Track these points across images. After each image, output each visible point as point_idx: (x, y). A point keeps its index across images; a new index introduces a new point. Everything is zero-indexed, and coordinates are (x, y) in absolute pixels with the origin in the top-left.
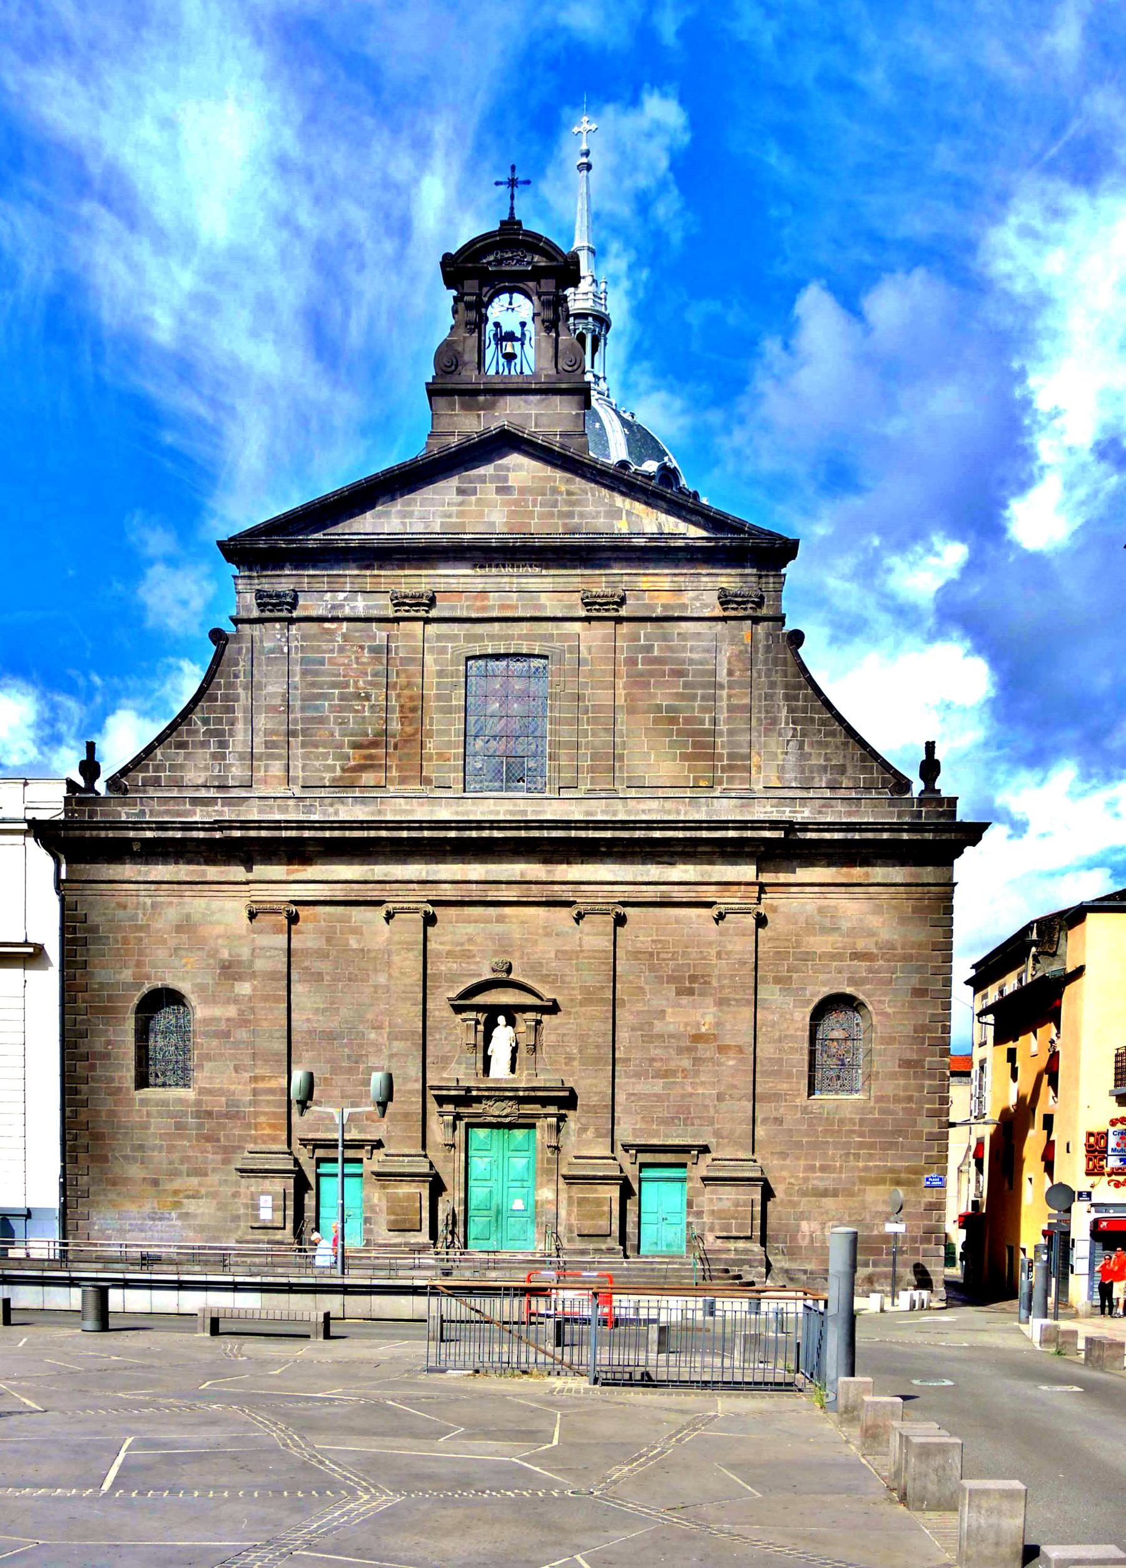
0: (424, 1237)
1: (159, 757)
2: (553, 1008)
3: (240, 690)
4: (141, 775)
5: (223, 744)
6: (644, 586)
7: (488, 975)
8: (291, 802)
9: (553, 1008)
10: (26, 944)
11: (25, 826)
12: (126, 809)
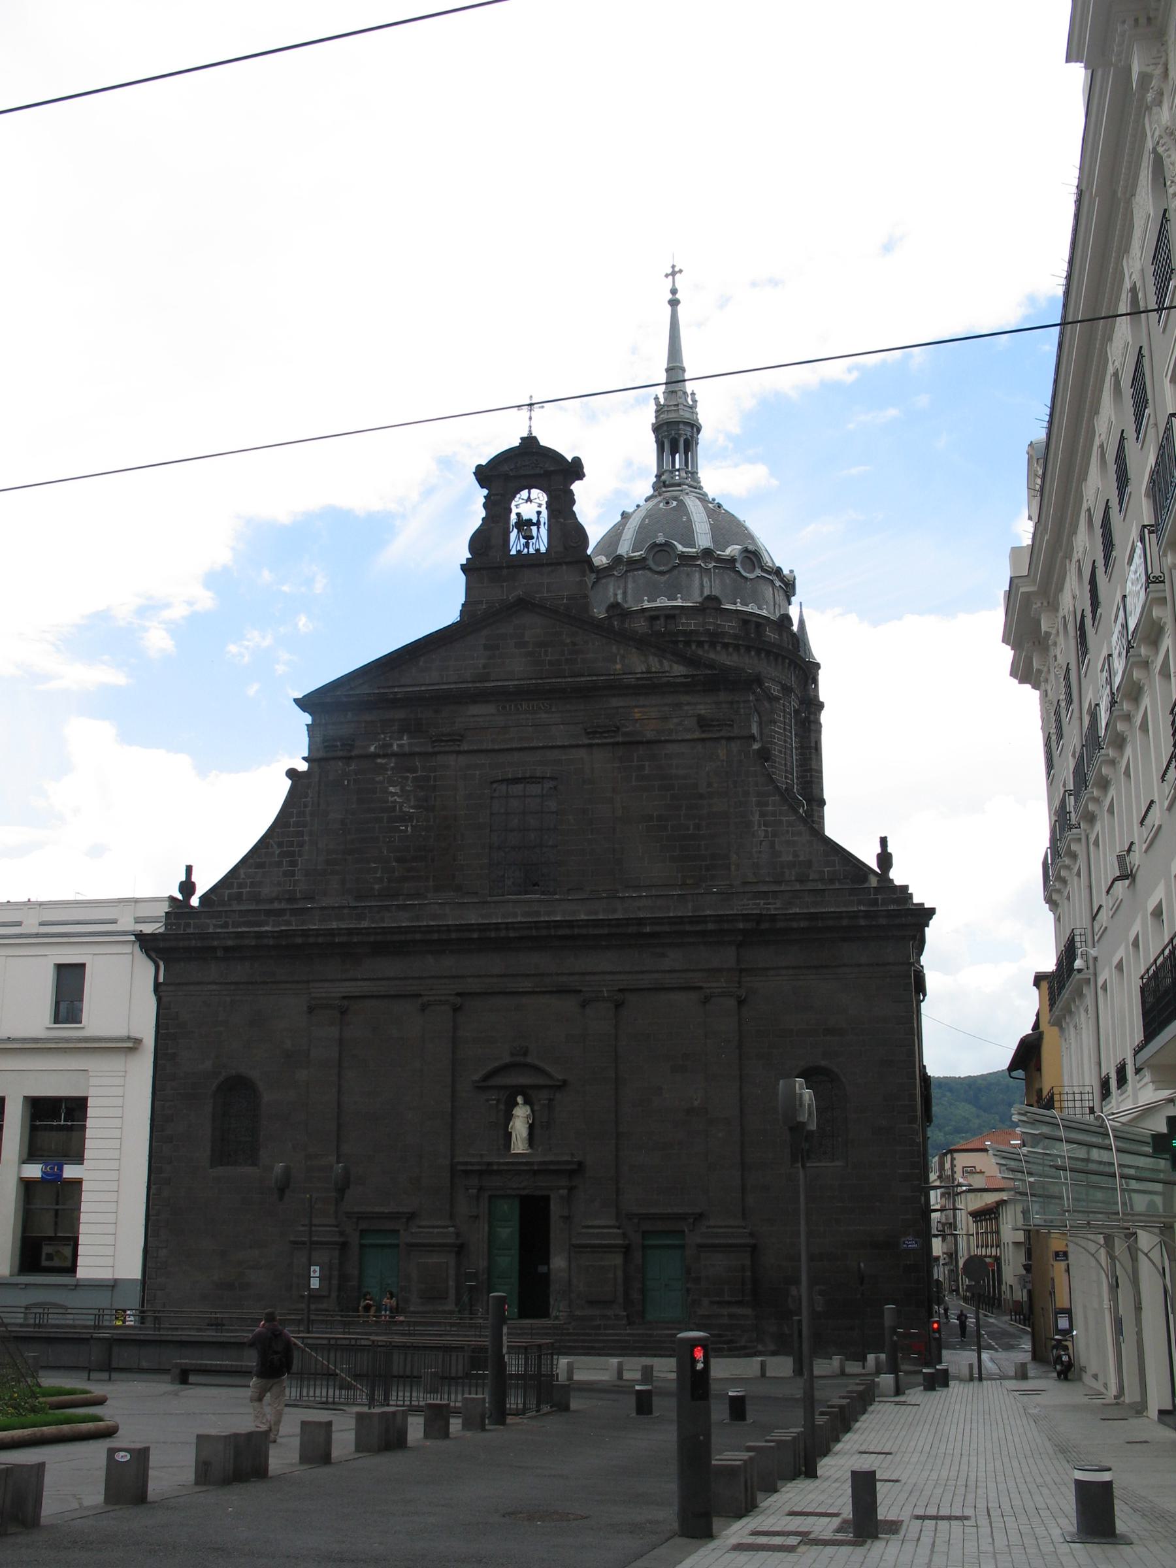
0: (450, 1306)
1: (243, 876)
2: (563, 1085)
3: (308, 819)
4: (227, 892)
5: (293, 864)
6: (637, 716)
7: (507, 1059)
8: (346, 911)
9: (563, 1085)
10: (129, 1038)
11: (133, 938)
12: (214, 921)
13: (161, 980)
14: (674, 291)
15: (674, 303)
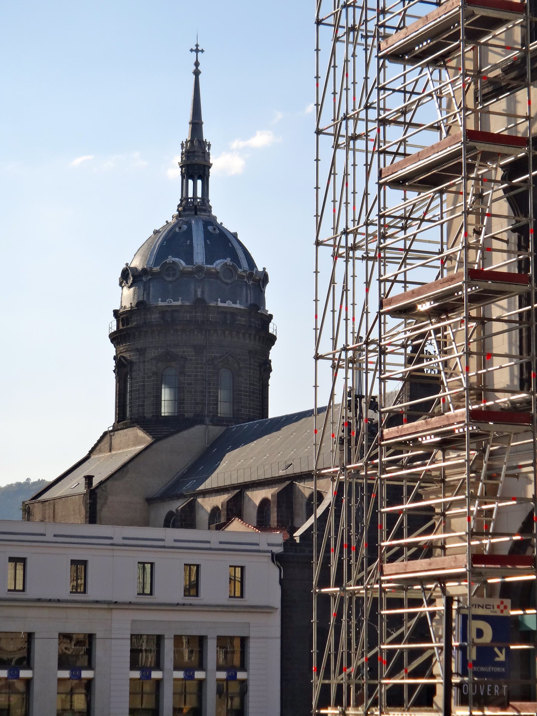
13: (282, 577)
14: (197, 64)
15: (197, 73)
